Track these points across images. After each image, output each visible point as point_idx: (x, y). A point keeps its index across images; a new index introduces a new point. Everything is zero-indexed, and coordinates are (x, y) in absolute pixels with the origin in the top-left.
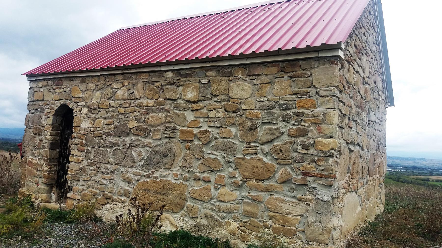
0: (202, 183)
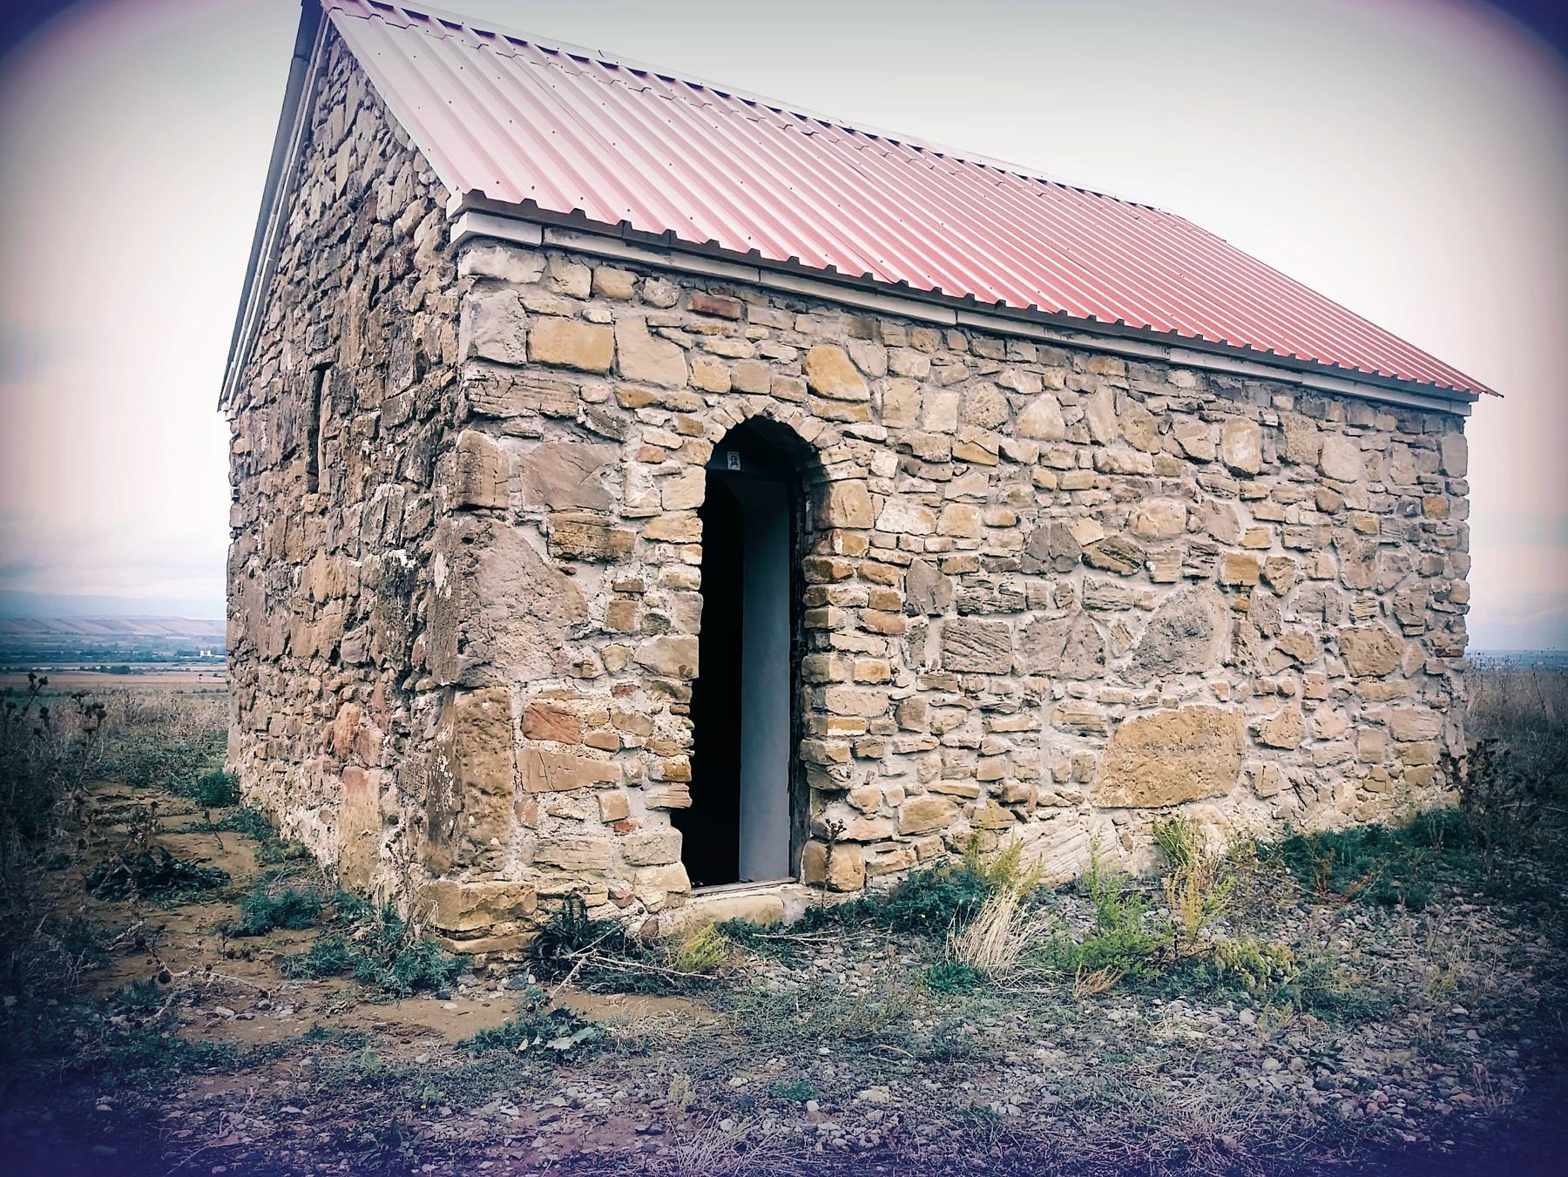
0: (1275, 699)
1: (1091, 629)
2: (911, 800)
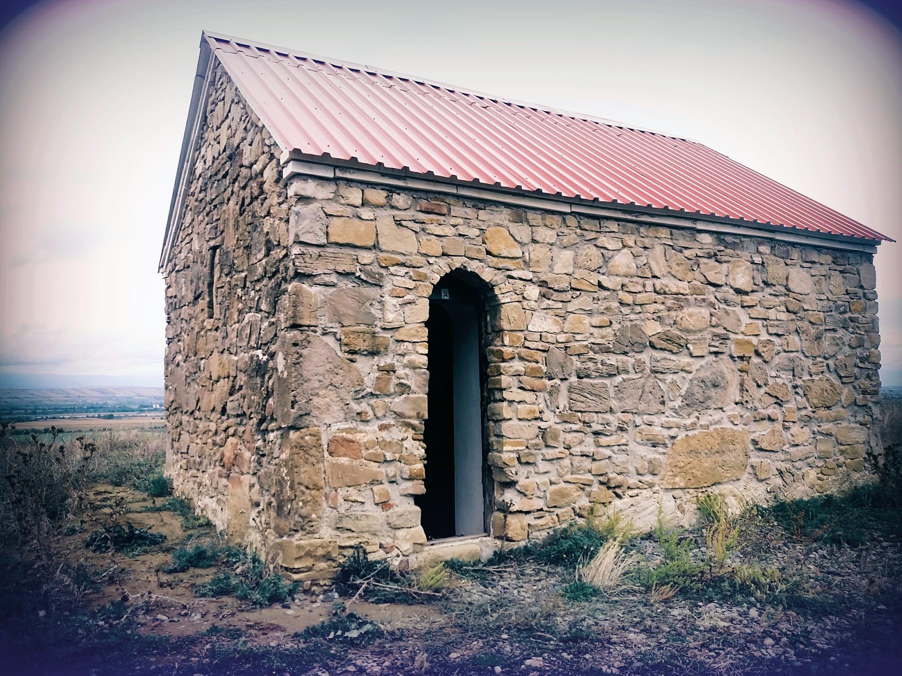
0: (766, 423)
1: (656, 384)
2: (554, 487)
